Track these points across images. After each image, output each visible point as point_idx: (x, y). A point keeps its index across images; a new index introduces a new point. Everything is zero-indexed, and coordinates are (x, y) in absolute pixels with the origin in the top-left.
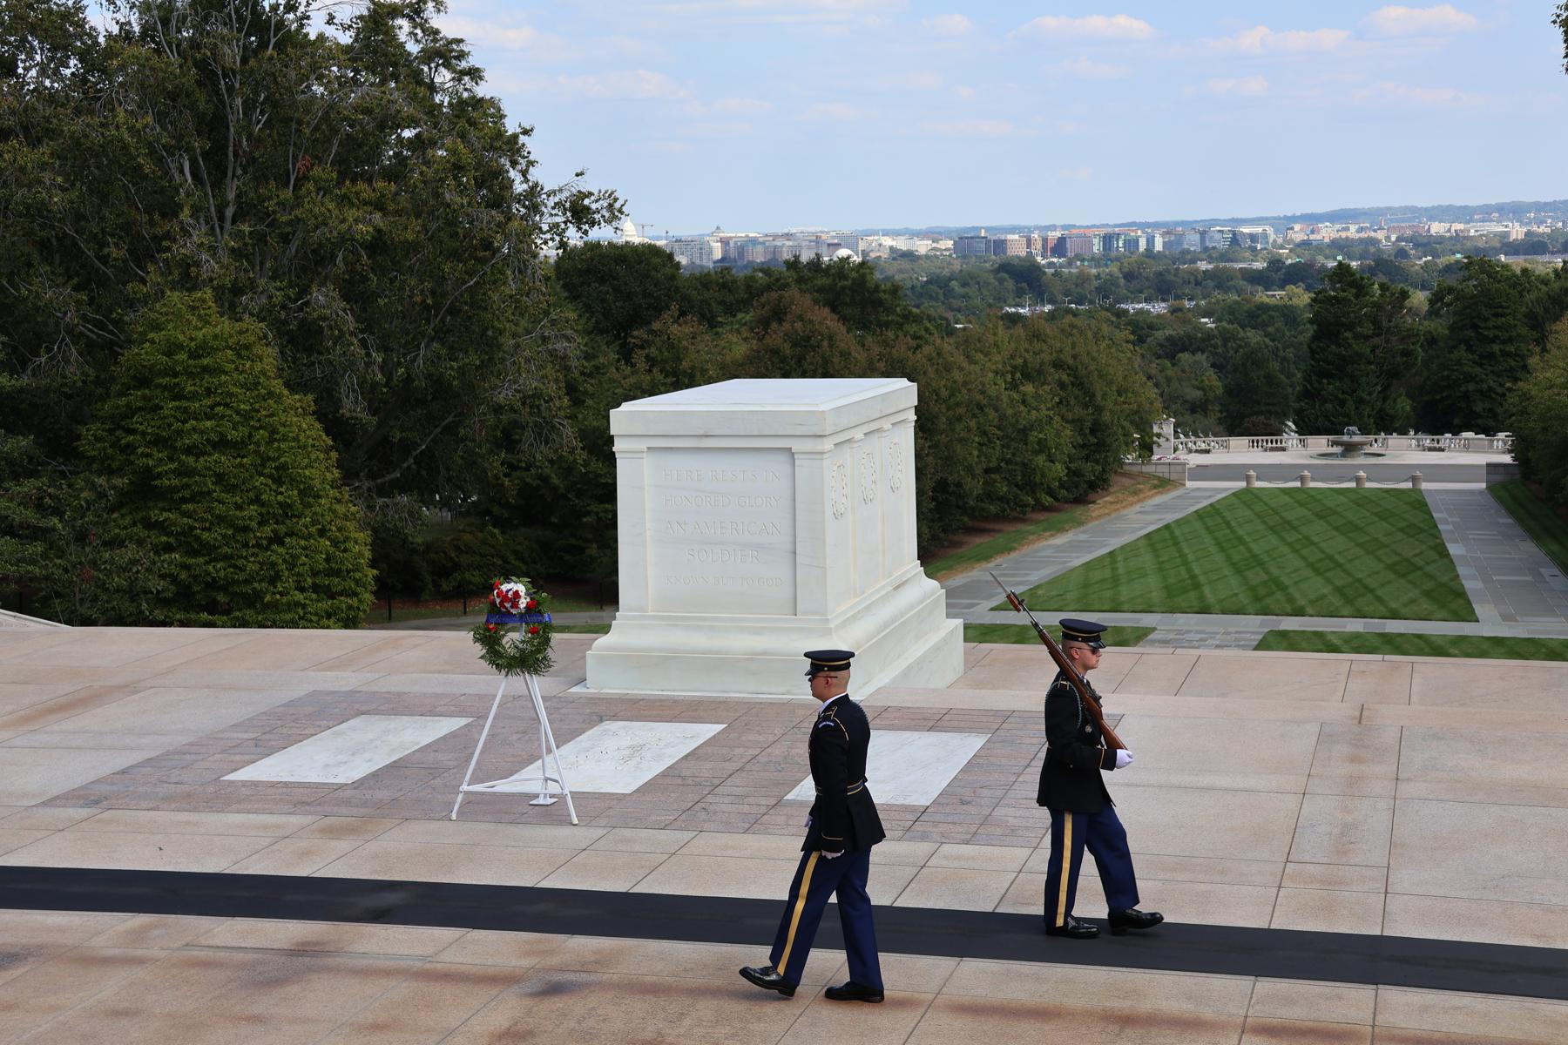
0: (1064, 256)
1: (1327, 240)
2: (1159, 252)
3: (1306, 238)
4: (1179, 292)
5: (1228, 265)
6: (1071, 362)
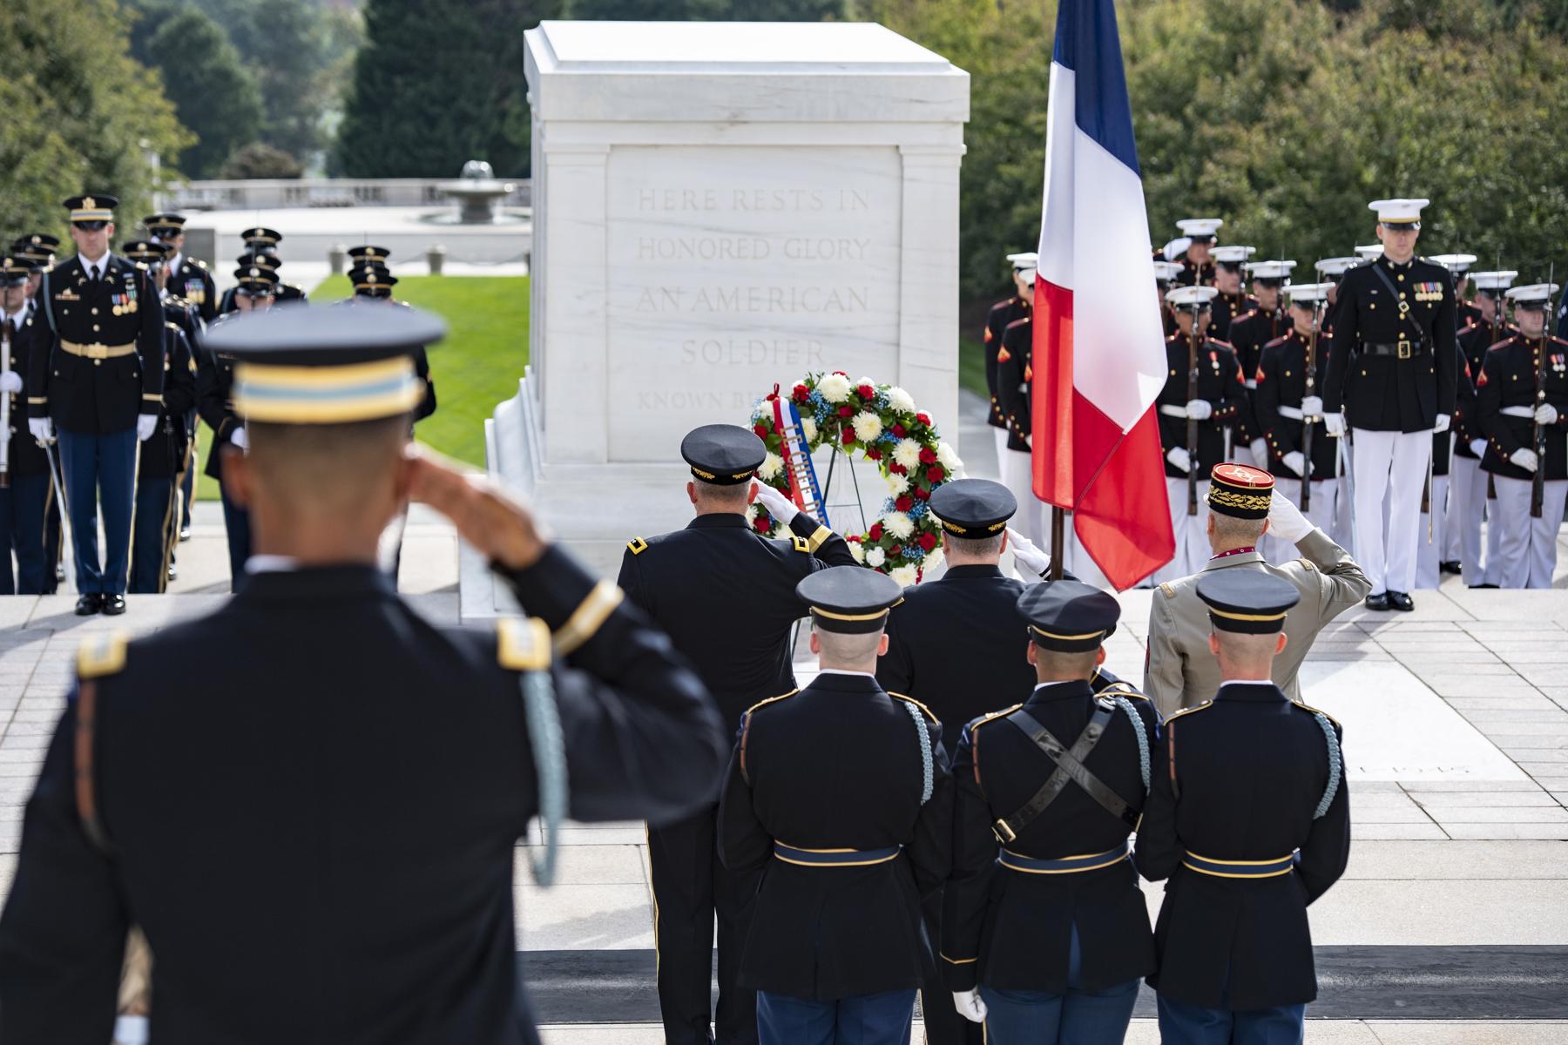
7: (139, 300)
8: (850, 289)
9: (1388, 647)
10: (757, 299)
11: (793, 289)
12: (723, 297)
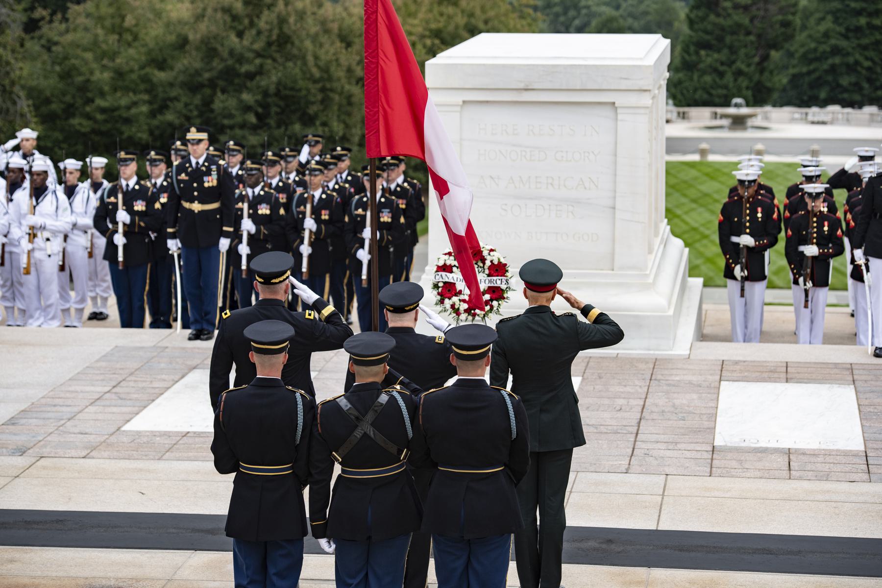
7: (218, 180)
8: (590, 178)
10: (540, 182)
11: (559, 178)
12: (522, 181)
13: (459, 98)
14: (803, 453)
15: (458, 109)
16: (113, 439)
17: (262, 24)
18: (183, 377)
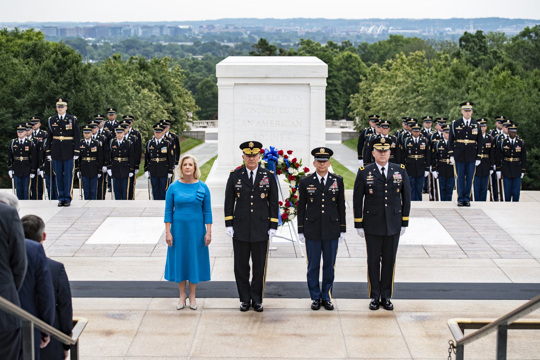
0: (95, 37)
1: (218, 33)
2: (141, 36)
3: (208, 31)
4: (153, 55)
5: (175, 43)
6: (160, 80)
9: (434, 214)
13: (232, 82)
14: (430, 247)
15: (232, 87)
16: (83, 248)
17: (66, 75)
18: (104, 220)
